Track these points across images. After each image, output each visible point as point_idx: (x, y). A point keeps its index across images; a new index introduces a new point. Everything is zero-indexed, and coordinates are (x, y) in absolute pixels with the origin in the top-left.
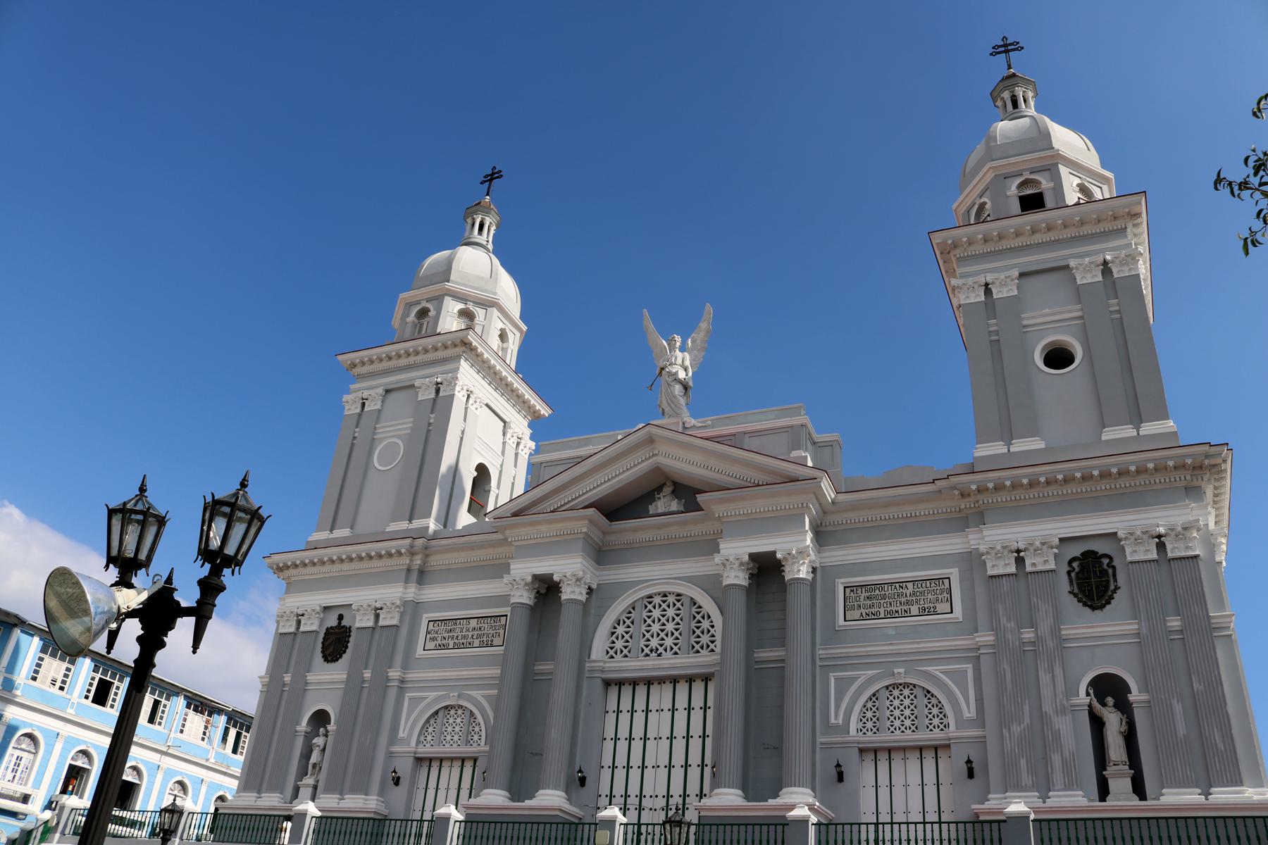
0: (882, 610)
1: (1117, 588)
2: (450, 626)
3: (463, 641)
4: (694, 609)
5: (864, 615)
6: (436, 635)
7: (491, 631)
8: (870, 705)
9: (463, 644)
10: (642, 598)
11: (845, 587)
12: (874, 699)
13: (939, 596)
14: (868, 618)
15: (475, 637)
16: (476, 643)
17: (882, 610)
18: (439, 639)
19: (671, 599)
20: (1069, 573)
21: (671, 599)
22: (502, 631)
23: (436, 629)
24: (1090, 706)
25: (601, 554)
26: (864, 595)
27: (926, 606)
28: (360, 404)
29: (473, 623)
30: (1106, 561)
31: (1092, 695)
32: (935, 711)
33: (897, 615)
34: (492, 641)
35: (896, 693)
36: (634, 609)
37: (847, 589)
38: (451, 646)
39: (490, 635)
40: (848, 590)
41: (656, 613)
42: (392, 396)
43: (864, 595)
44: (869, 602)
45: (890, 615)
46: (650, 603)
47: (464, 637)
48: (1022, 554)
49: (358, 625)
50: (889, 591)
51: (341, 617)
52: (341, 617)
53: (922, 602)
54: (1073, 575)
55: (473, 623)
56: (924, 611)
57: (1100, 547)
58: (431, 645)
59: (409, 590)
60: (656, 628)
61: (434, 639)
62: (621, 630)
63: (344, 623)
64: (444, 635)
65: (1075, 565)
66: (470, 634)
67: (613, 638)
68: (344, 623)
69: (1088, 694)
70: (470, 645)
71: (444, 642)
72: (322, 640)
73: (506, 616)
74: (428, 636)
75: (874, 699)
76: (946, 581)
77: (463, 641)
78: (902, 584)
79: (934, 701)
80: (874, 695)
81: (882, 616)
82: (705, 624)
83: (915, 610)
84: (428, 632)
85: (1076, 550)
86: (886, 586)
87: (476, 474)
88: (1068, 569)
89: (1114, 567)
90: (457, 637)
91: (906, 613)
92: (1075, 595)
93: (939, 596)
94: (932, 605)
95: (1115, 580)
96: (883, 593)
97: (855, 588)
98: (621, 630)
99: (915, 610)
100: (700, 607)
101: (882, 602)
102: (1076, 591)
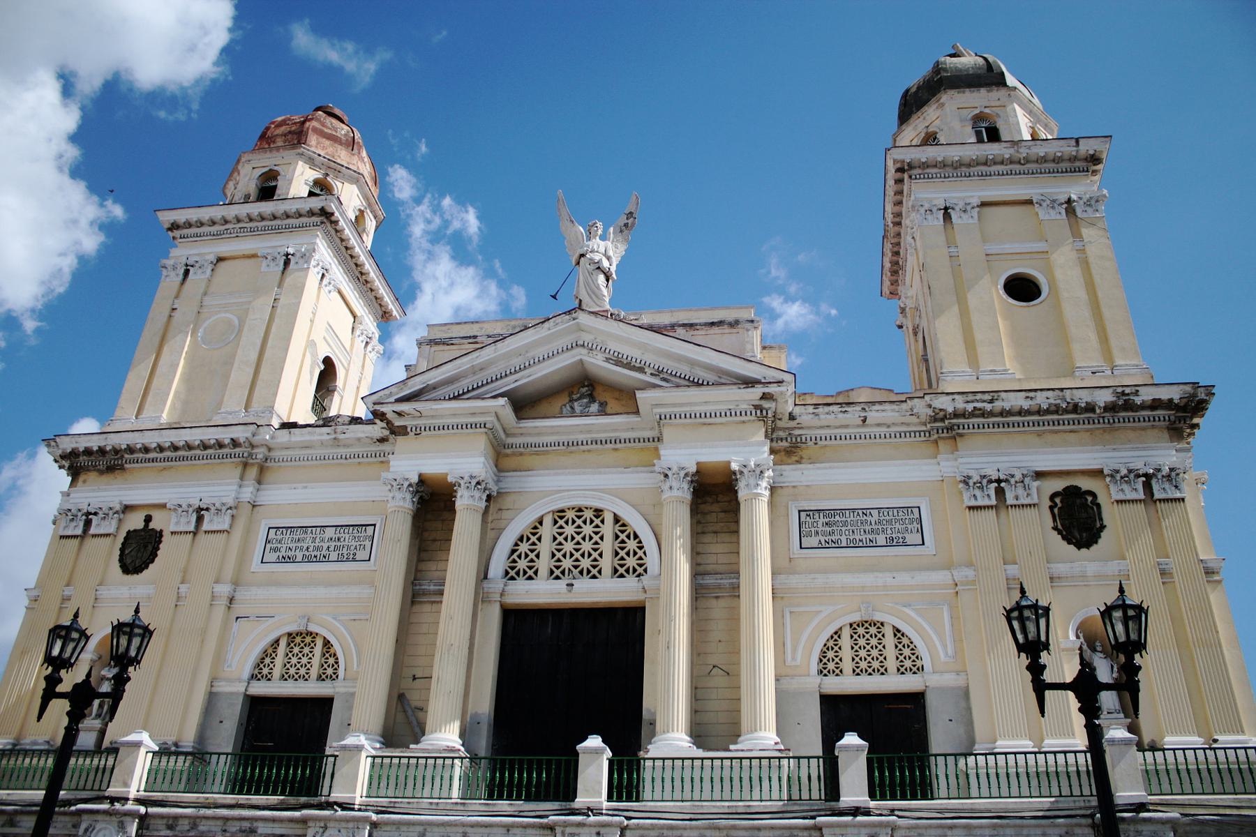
0: (843, 538)
1: (1103, 527)
2: (298, 534)
3: (315, 553)
4: (617, 527)
5: (823, 542)
6: (279, 546)
7: (354, 543)
8: (831, 643)
9: (315, 557)
10: (553, 512)
11: (799, 511)
12: (836, 637)
13: (909, 527)
14: (827, 545)
15: (332, 549)
16: (334, 556)
17: (843, 538)
18: (283, 550)
19: (588, 514)
20: (1051, 508)
22: (368, 544)
23: (279, 537)
24: (1081, 649)
26: (822, 520)
27: (894, 536)
28: (182, 271)
29: (330, 532)
30: (1090, 499)
31: (1082, 637)
32: (907, 652)
33: (861, 544)
34: (355, 554)
35: (861, 631)
36: (541, 523)
37: (802, 513)
38: (299, 559)
39: (352, 548)
40: (803, 514)
42: (222, 265)
43: (822, 520)
44: (828, 529)
46: (561, 518)
47: (318, 549)
48: (1003, 485)
49: (173, 528)
50: (850, 518)
51: (148, 519)
52: (148, 519)
53: (889, 532)
54: (1056, 510)
55: (330, 532)
56: (891, 542)
57: (1085, 484)
59: (244, 490)
61: (276, 550)
62: (524, 547)
63: (151, 526)
64: (291, 546)
65: (1058, 500)
66: (325, 546)
67: (515, 556)
68: (151, 526)
69: (1078, 637)
70: (325, 559)
71: (290, 554)
72: (122, 540)
73: (375, 525)
74: (268, 546)
75: (836, 637)
76: (915, 511)
77: (315, 553)
78: (865, 511)
79: (905, 641)
80: (836, 633)
81: (844, 544)
82: (632, 545)
83: (881, 540)
84: (267, 541)
85: (1059, 485)
86: (847, 512)
87: (322, 367)
88: (1050, 503)
89: (1098, 506)
90: (308, 548)
91: (872, 545)
92: (1060, 532)
93: (909, 527)
94: (900, 536)
95: (1101, 519)
96: (844, 519)
97: (811, 513)
98: (524, 547)
99: (881, 540)
100: (624, 525)
101: (843, 529)
102: (1060, 527)
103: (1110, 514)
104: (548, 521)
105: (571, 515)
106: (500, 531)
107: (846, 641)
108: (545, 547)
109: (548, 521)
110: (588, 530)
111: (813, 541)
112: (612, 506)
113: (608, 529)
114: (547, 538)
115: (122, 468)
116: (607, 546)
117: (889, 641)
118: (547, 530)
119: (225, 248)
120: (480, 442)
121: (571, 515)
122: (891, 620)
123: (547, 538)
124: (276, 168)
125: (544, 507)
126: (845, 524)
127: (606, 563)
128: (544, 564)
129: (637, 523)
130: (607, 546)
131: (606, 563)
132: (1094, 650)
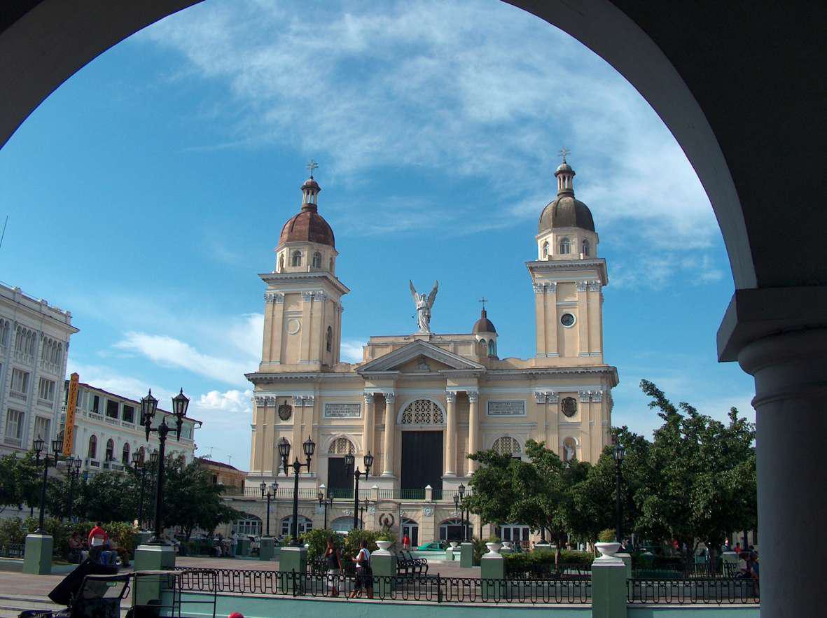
19: (426, 402)
21: (426, 402)
24: (564, 448)
25: (399, 384)
26: (495, 406)
41: (420, 407)
43: (495, 406)
45: (504, 413)
52: (286, 402)
56: (515, 413)
58: (328, 415)
60: (420, 413)
78: (508, 403)
82: (439, 412)
85: (565, 396)
98: (407, 413)
103: (579, 407)
104: (414, 404)
105: (420, 402)
106: (399, 408)
107: (500, 442)
108: (413, 413)
109: (414, 404)
110: (426, 407)
111: (492, 412)
112: (432, 401)
113: (432, 407)
114: (414, 410)
115: (272, 383)
116: (432, 413)
117: (512, 443)
118: (414, 407)
119: (289, 290)
120: (392, 383)
121: (420, 402)
122: (513, 436)
123: (414, 410)
124: (300, 250)
125: (413, 400)
126: (501, 407)
127: (432, 418)
128: (413, 418)
129: (440, 406)
130: (432, 413)
131: (432, 418)
132: (568, 446)
